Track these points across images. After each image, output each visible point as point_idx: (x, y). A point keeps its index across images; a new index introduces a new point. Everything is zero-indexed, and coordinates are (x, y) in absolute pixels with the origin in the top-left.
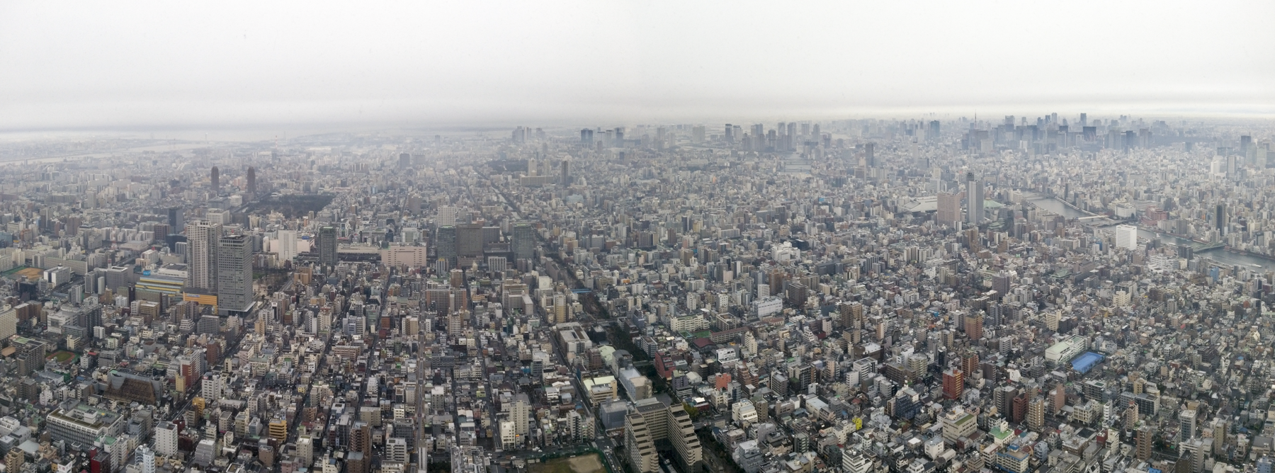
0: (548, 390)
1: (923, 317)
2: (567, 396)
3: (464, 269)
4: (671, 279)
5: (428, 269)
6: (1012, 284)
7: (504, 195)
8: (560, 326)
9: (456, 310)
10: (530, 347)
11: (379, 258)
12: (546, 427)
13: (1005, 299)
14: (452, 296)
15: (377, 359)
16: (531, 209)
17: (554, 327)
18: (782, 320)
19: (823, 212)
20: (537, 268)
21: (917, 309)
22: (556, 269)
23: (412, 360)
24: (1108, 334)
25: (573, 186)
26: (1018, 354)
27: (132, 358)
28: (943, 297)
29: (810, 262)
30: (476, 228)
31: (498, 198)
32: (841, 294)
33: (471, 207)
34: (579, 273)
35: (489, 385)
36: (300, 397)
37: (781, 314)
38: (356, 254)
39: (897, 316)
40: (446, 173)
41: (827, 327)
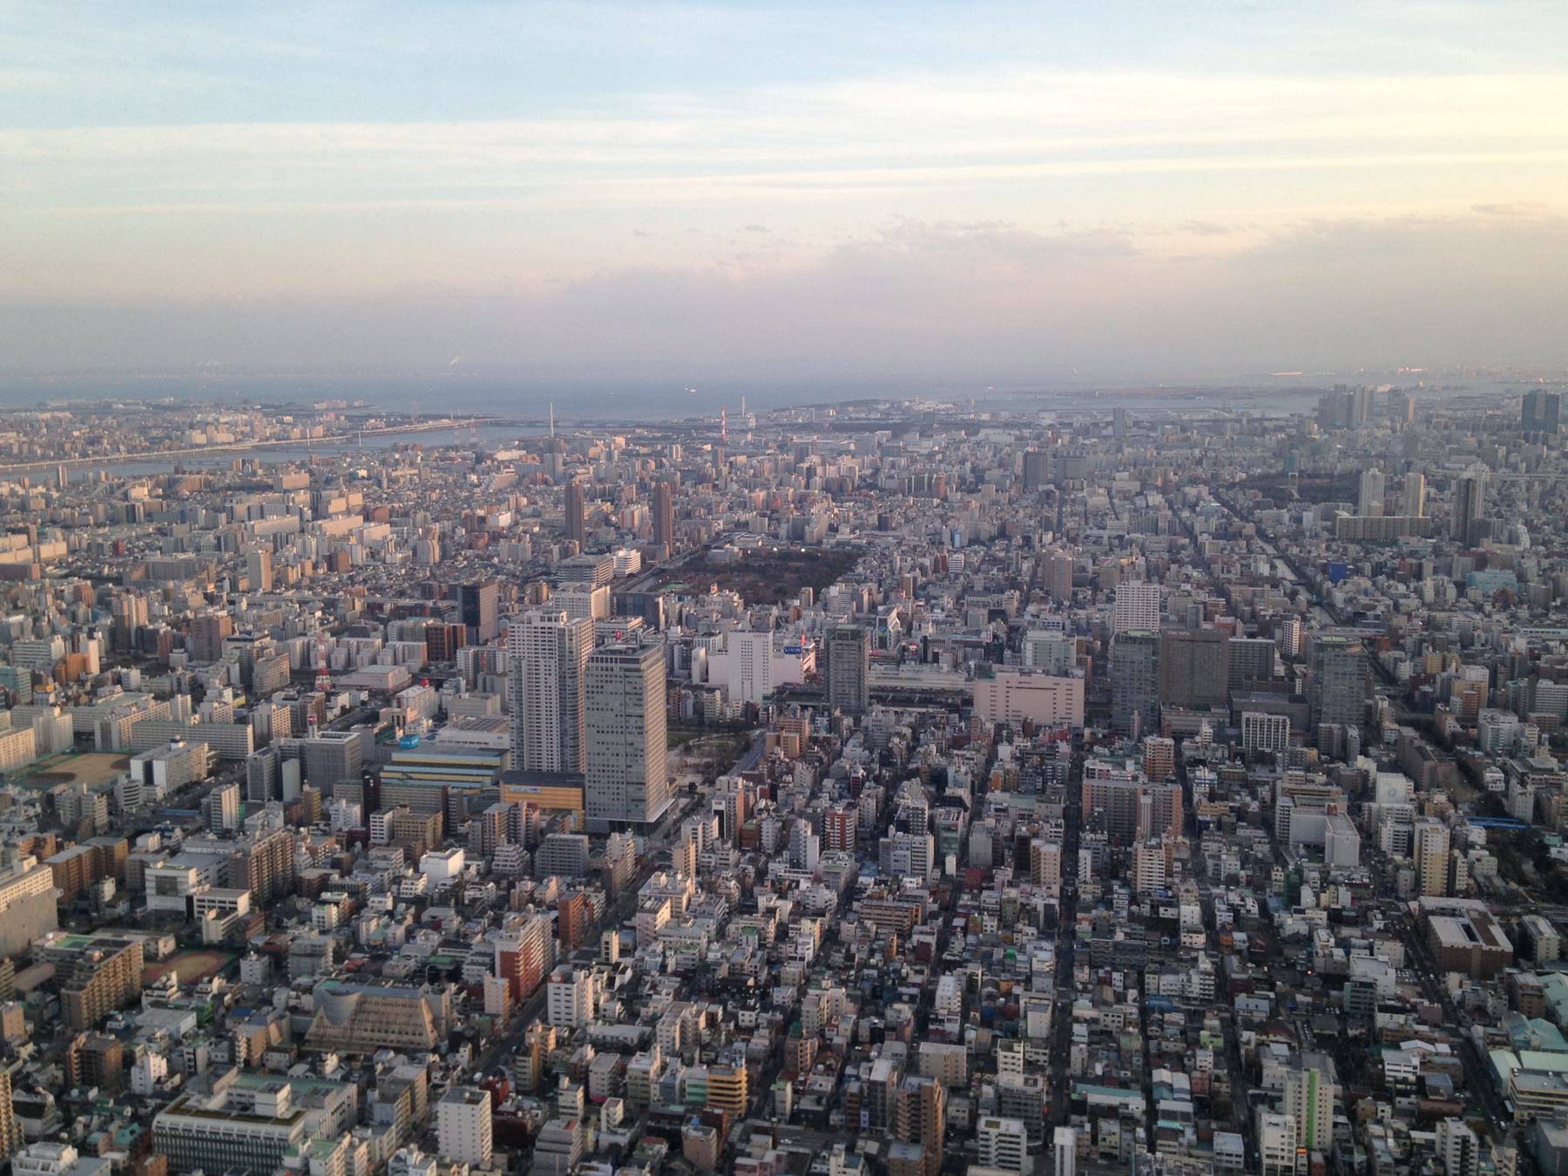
0: (1388, 1055)
2: (1440, 1081)
3: (1178, 737)
5: (1087, 731)
7: (1289, 563)
8: (1430, 902)
9: (1155, 833)
10: (1344, 944)
11: (969, 702)
12: (1377, 1144)
14: (1146, 800)
15: (960, 935)
16: (1363, 600)
17: (1413, 905)
20: (1372, 750)
22: (1425, 757)
23: (1045, 944)
25: (1487, 545)
27: (374, 947)
30: (1210, 640)
31: (1273, 567)
33: (1199, 586)
34: (1492, 777)
35: (1233, 1021)
36: (779, 1016)
38: (912, 691)
40: (1140, 502)
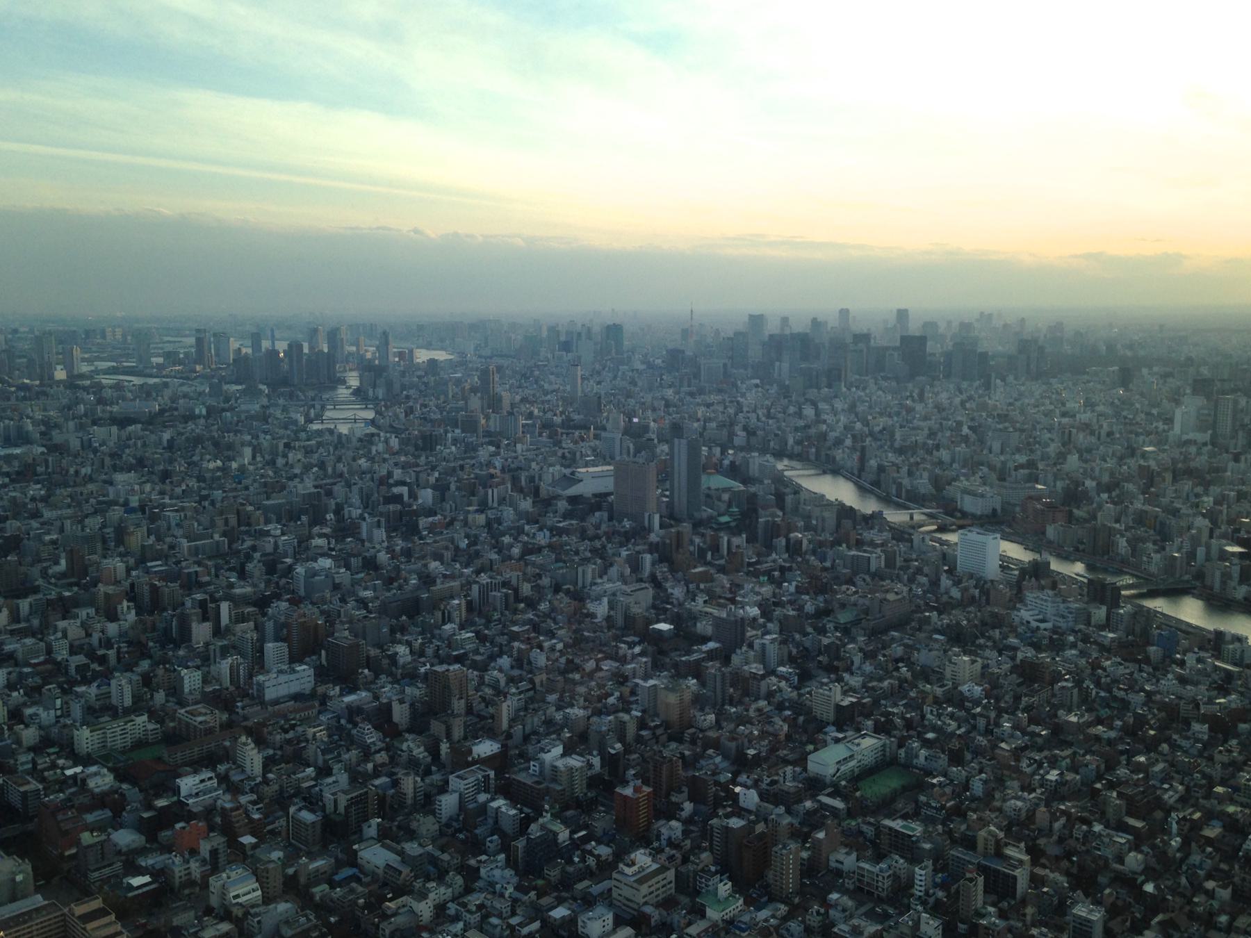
1: (582, 690)
4: (73, 650)
6: (750, 633)
13: (736, 659)
18: (313, 707)
19: (398, 499)
21: (571, 676)
24: (930, 735)
26: (757, 761)
28: (621, 652)
29: (368, 594)
32: (430, 651)
37: (313, 695)
39: (534, 688)
41: (400, 713)
